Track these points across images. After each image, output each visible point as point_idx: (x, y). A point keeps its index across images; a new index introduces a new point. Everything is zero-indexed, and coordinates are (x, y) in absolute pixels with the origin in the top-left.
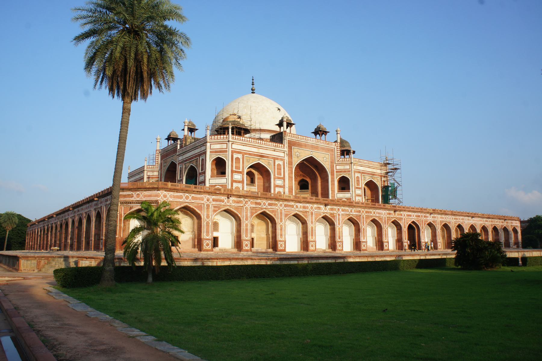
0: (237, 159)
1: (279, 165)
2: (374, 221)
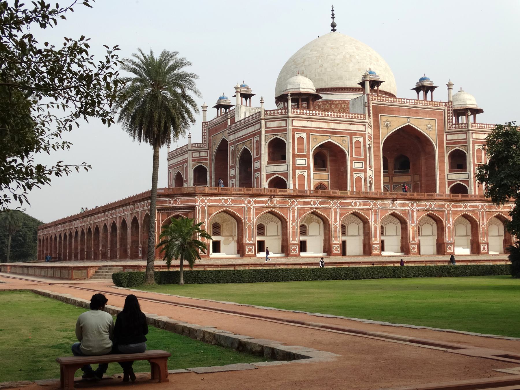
0: (301, 138)
1: (358, 142)
2: (466, 216)
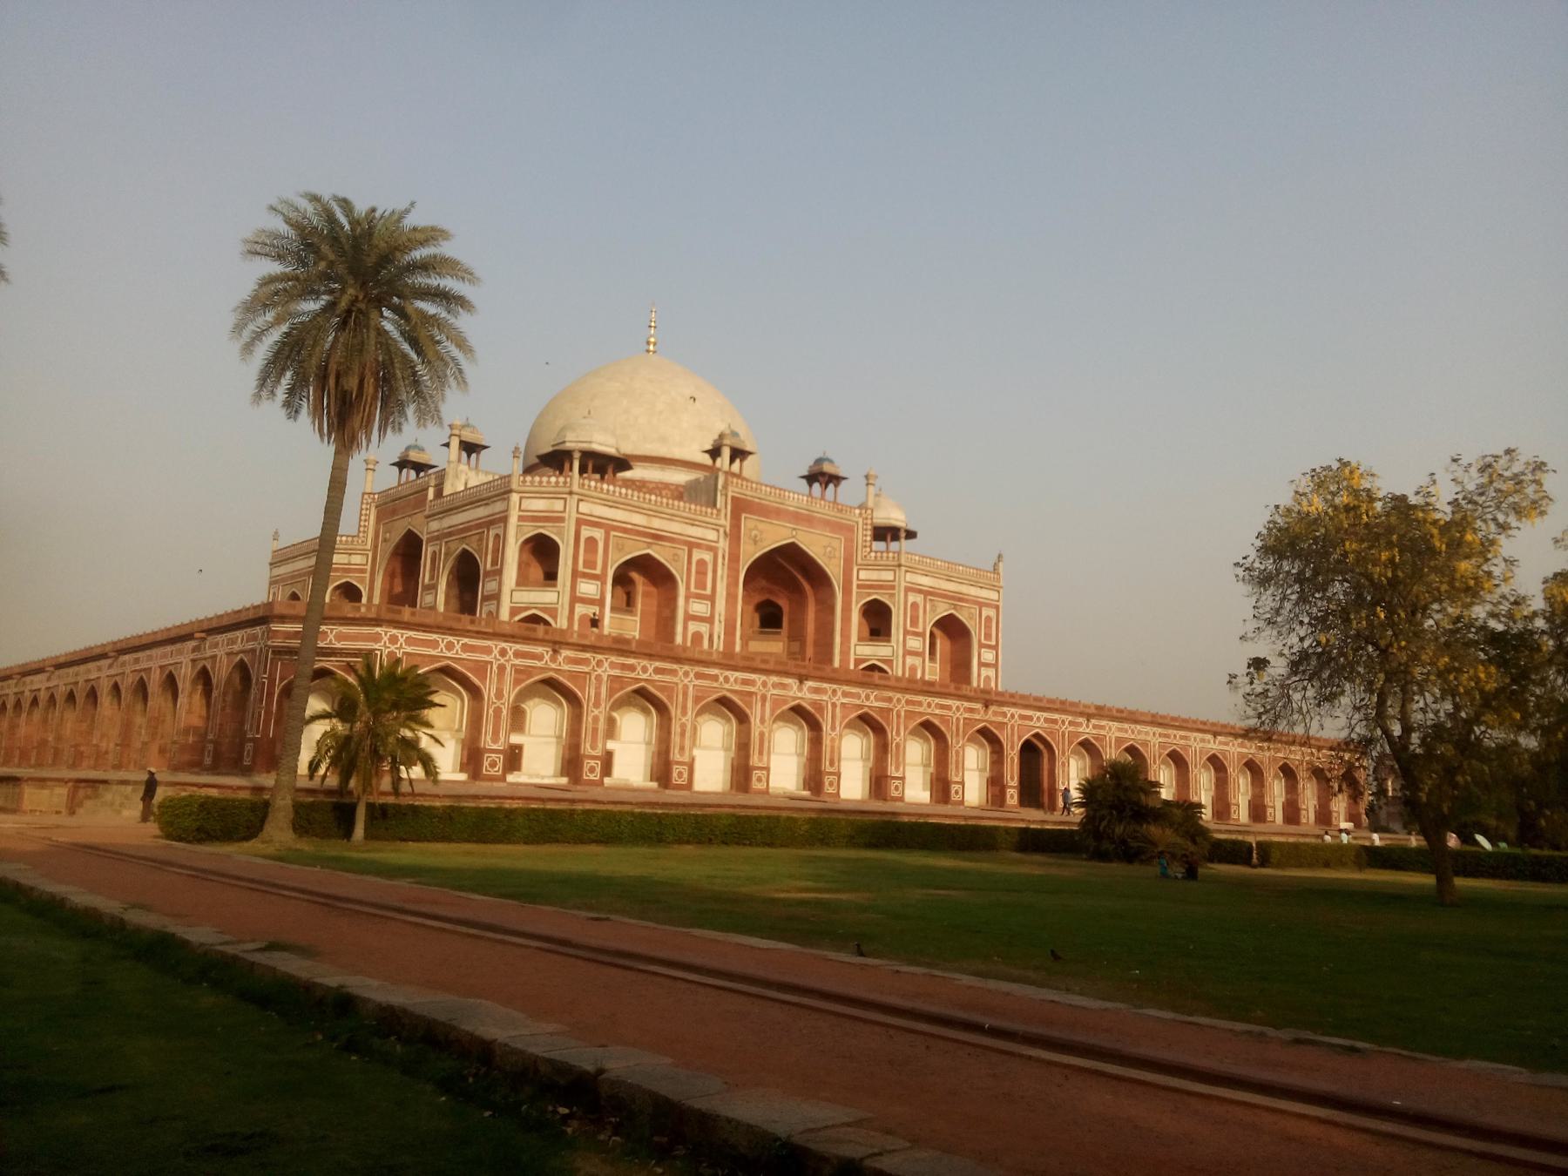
1: (701, 563)
2: (928, 726)
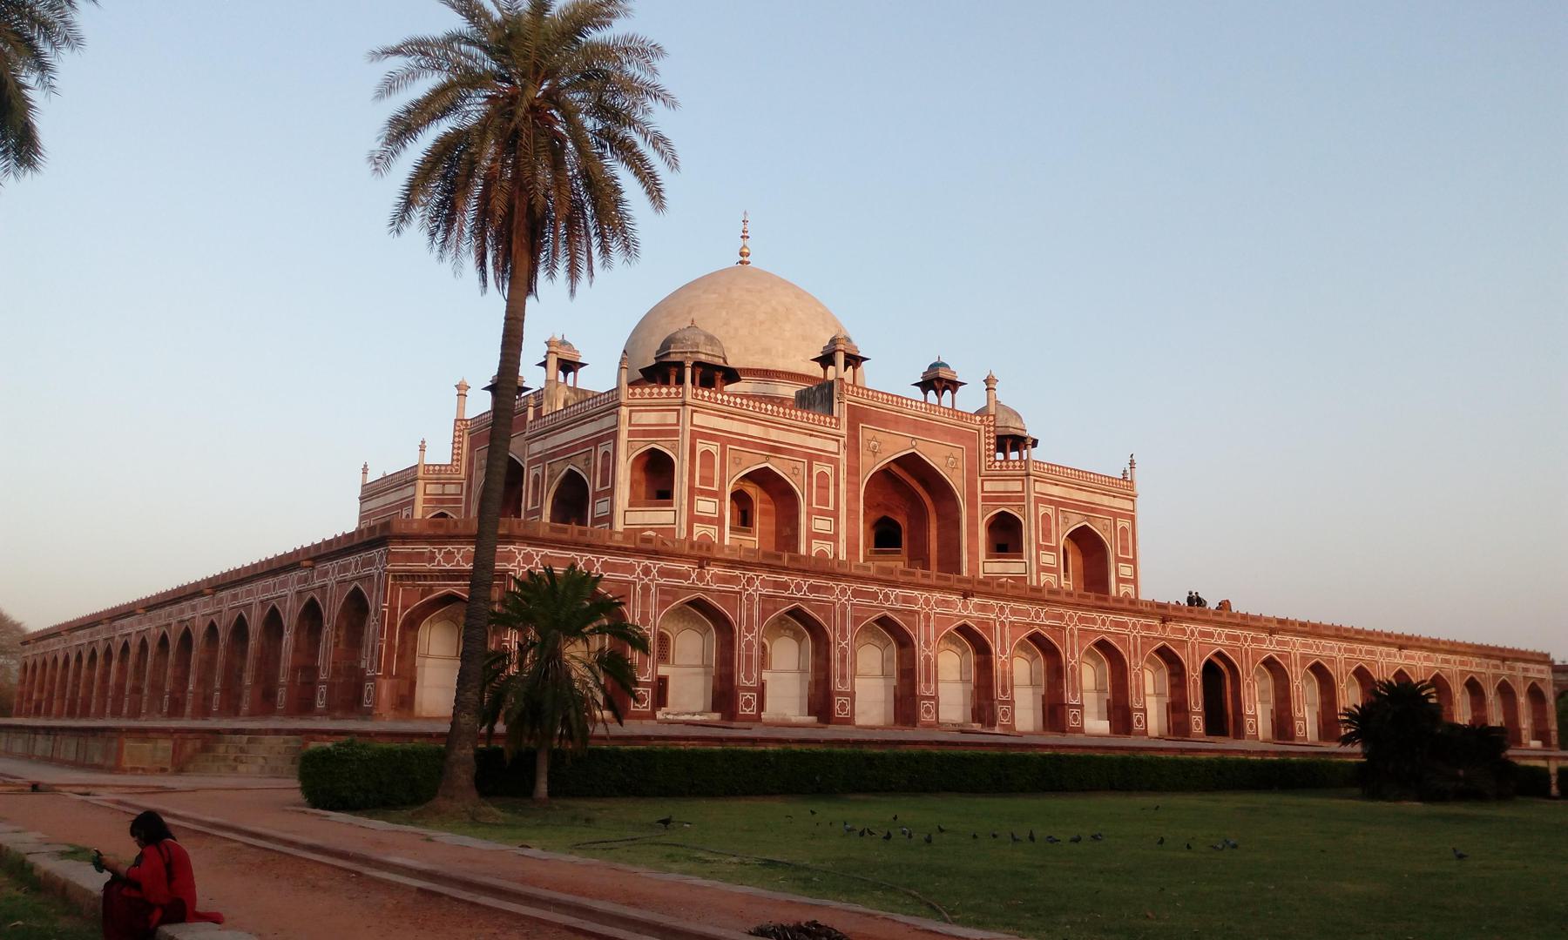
0: (707, 455)
1: (822, 475)
2: (1103, 645)
